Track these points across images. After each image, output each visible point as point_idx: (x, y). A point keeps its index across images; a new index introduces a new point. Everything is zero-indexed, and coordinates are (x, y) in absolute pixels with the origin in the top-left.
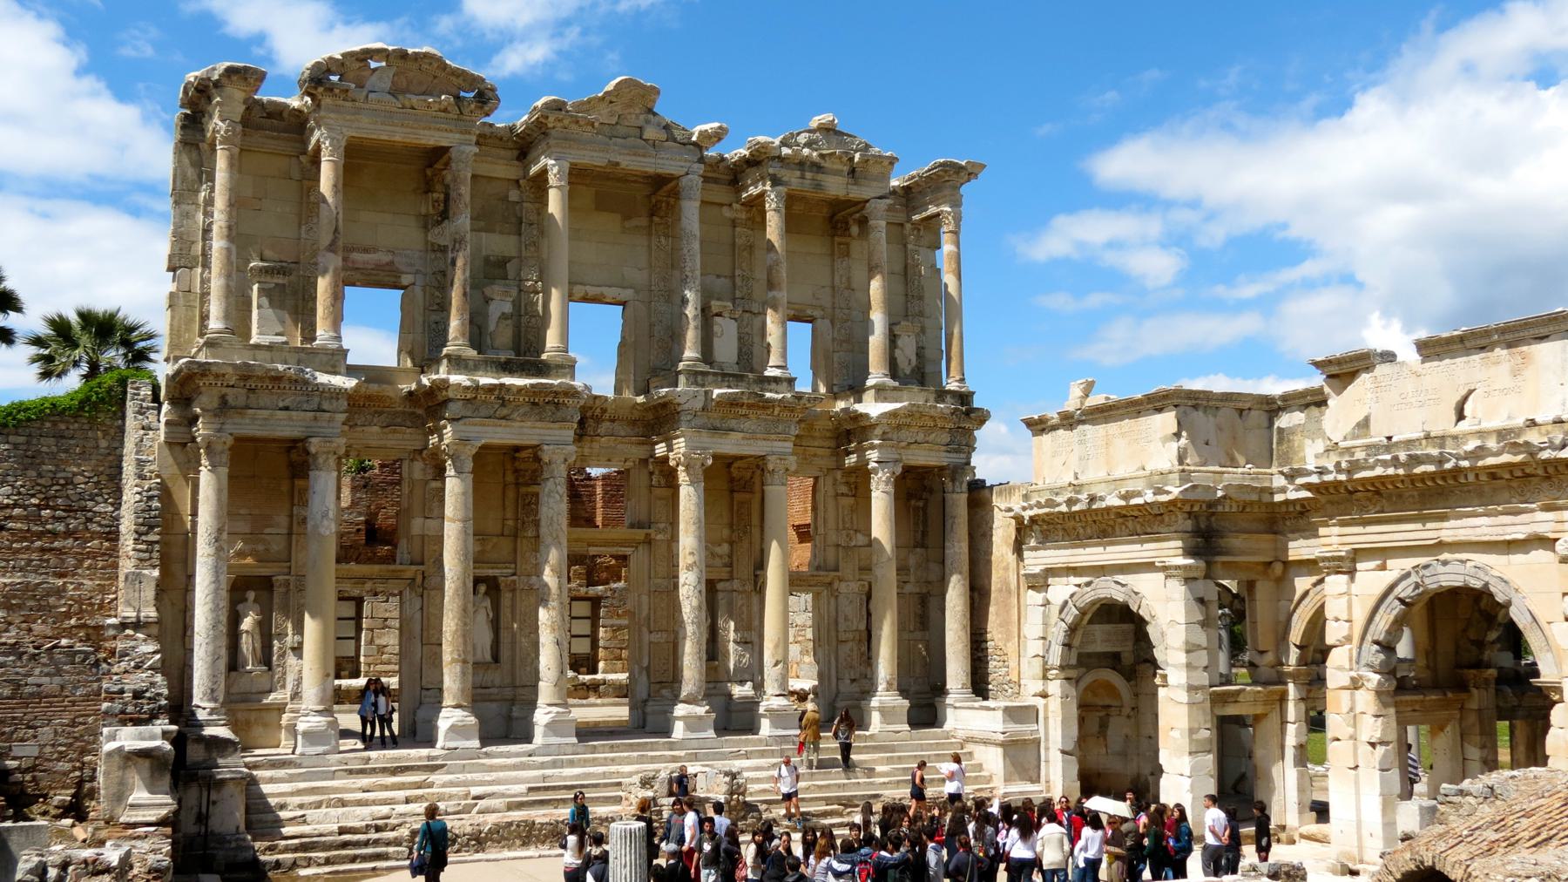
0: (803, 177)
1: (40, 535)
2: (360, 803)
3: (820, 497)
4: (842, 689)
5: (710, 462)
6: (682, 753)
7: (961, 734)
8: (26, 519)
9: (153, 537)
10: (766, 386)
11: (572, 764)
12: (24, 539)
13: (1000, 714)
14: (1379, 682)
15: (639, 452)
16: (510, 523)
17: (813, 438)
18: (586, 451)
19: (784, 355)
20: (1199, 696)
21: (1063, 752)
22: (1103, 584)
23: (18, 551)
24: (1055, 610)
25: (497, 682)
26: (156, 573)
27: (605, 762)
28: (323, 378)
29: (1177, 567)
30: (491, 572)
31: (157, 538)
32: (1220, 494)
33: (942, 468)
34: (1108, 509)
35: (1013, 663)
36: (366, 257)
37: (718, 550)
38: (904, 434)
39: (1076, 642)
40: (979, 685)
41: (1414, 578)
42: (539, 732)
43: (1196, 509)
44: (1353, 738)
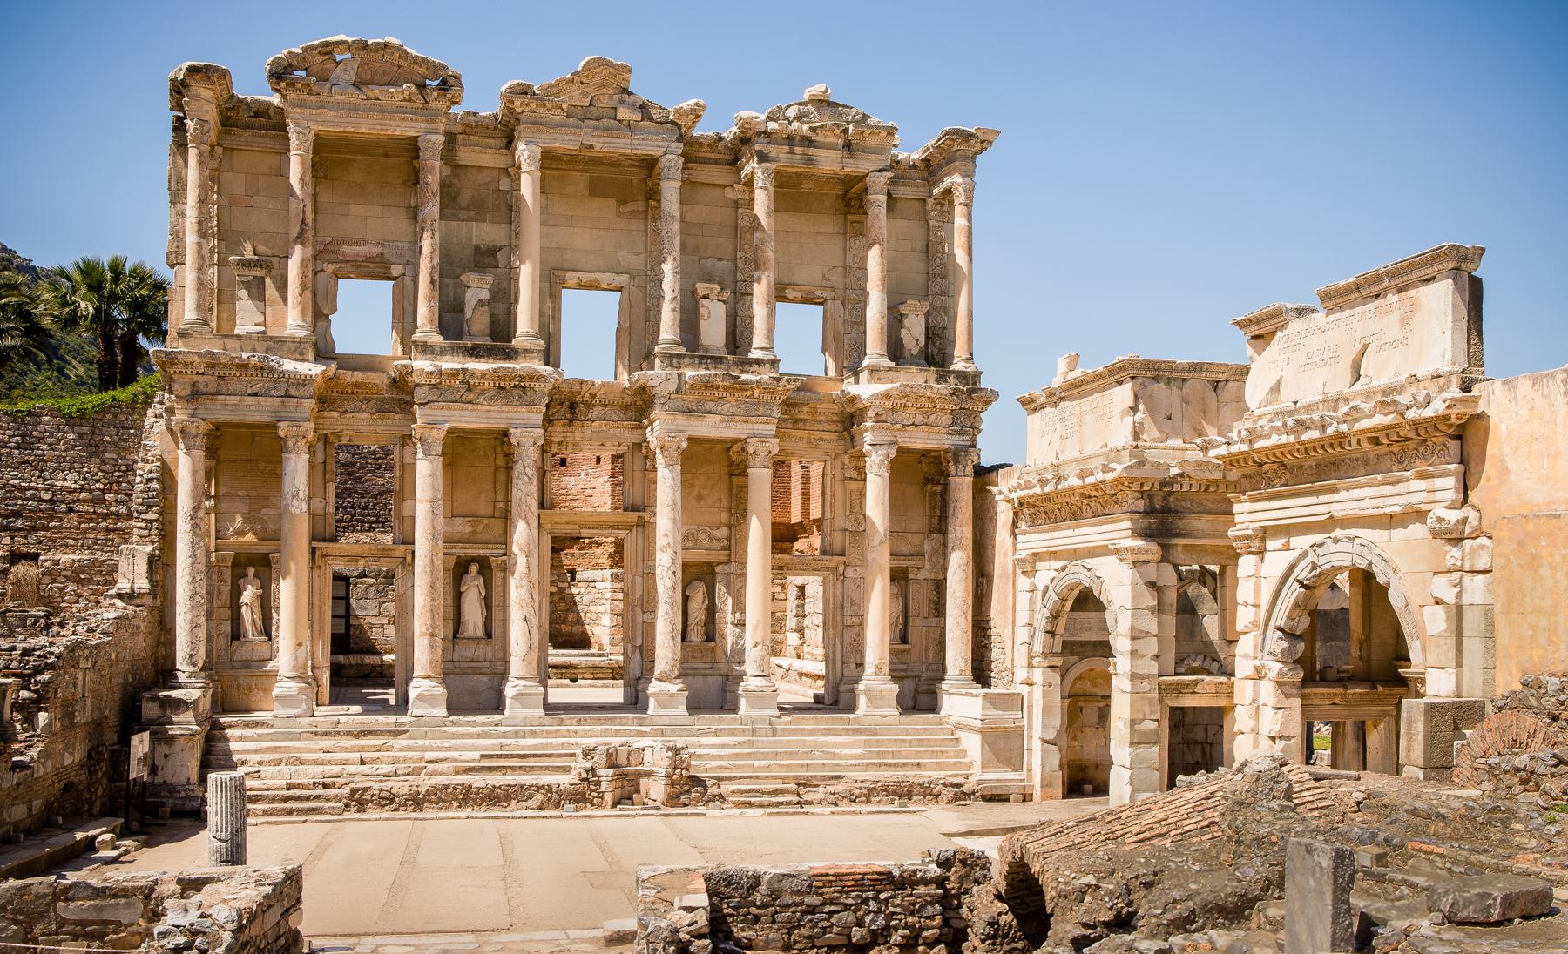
0: (792, 152)
1: (105, 517)
2: (316, 762)
3: (828, 481)
4: (846, 673)
5: (685, 444)
6: (647, 729)
7: (953, 720)
8: (92, 502)
9: (151, 516)
10: (747, 367)
11: (534, 734)
12: (92, 520)
13: (980, 700)
14: (1280, 673)
15: (632, 436)
16: (501, 505)
17: (819, 422)
18: (578, 436)
19: (770, 338)
20: (1146, 686)
21: (1044, 741)
22: (1074, 569)
23: (86, 531)
24: (1039, 594)
25: (489, 656)
26: (149, 548)
27: (568, 734)
28: (289, 365)
29: (1126, 550)
30: (482, 552)
31: (155, 516)
32: (1174, 472)
33: (946, 451)
34: (1072, 490)
35: (1008, 651)
36: (358, 249)
37: (717, 533)
38: (899, 416)
39: (1060, 629)
40: (981, 672)
41: (1310, 558)
42: (508, 702)
43: (1146, 488)
44: (1255, 731)
